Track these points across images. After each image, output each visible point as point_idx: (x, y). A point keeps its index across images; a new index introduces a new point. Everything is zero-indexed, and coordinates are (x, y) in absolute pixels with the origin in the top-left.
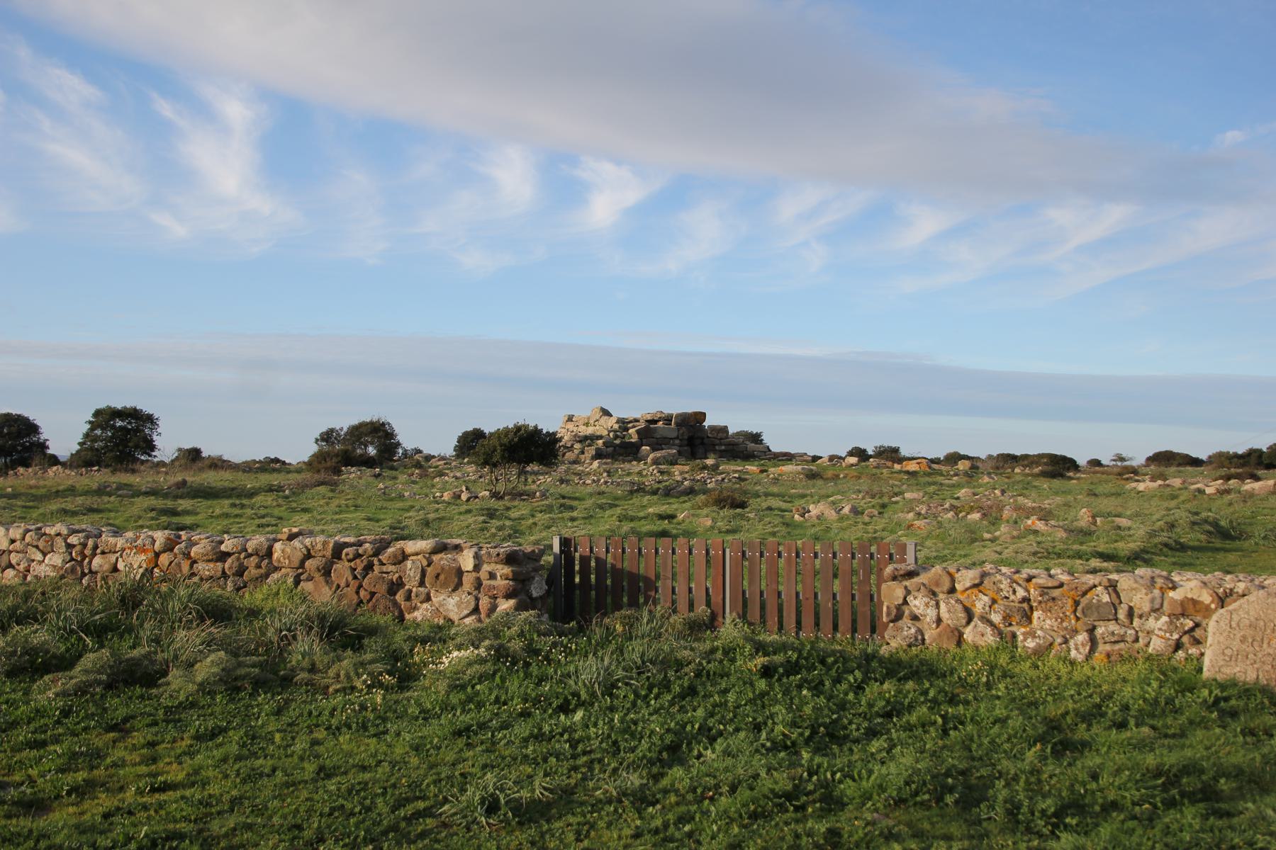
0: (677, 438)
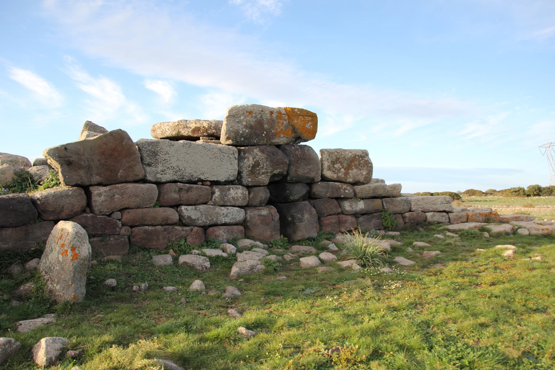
0: (238, 180)
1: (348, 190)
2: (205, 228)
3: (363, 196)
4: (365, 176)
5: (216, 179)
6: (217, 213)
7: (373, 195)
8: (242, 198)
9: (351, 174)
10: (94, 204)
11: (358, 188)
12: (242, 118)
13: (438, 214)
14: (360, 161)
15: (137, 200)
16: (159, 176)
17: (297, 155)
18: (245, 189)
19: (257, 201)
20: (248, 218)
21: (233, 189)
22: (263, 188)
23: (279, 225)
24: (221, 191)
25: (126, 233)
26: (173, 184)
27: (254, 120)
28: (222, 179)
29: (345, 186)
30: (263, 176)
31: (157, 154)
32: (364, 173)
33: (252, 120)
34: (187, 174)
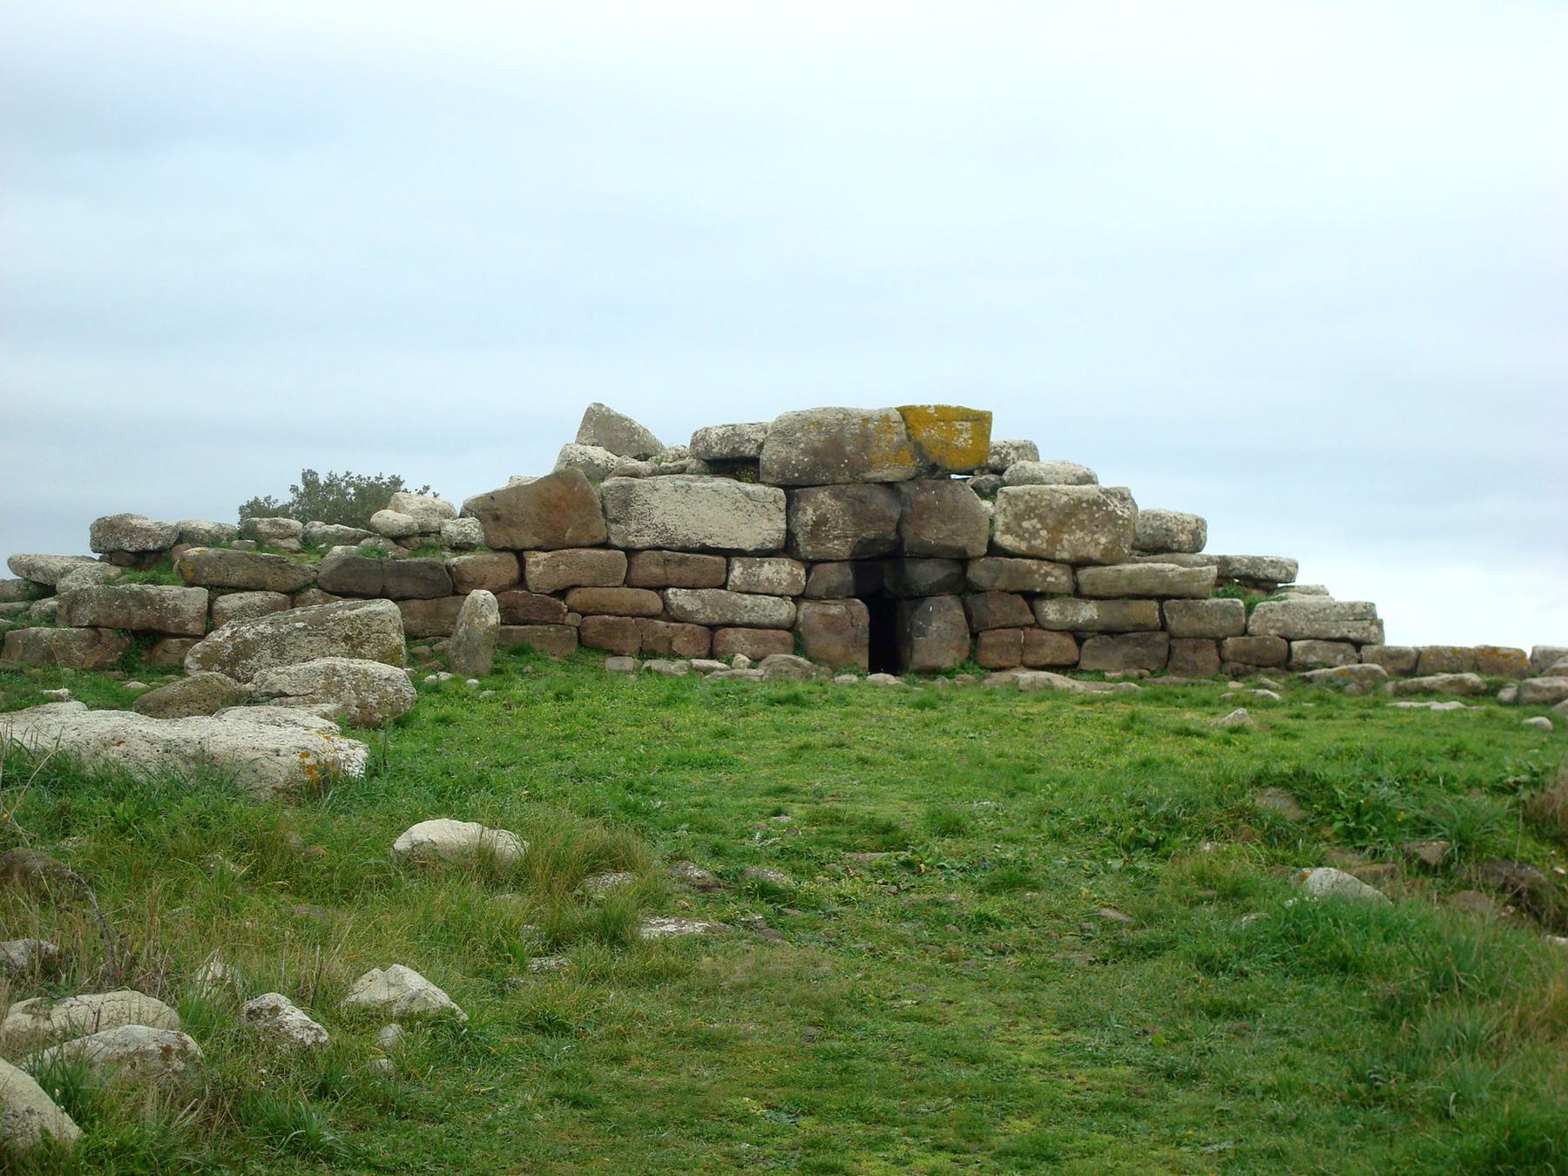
0: (787, 548)
1: (1058, 578)
2: (712, 628)
3: (1100, 592)
4: (1105, 549)
5: (736, 547)
6: (734, 604)
7: (1130, 591)
8: (789, 581)
9: (1065, 543)
10: (528, 577)
11: (1085, 574)
12: (798, 435)
13: (1326, 644)
14: (1092, 514)
15: (593, 573)
16: (631, 538)
17: (921, 502)
18: (798, 564)
19: (820, 588)
20: (801, 617)
21: (770, 564)
22: (835, 565)
23: (867, 635)
24: (743, 565)
25: (574, 623)
26: (656, 553)
27: (822, 438)
28: (749, 544)
29: (1046, 568)
30: (836, 542)
31: (629, 505)
32: (1103, 540)
33: (817, 439)
34: (680, 537)
